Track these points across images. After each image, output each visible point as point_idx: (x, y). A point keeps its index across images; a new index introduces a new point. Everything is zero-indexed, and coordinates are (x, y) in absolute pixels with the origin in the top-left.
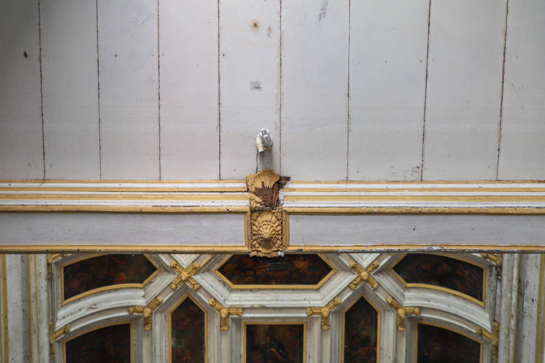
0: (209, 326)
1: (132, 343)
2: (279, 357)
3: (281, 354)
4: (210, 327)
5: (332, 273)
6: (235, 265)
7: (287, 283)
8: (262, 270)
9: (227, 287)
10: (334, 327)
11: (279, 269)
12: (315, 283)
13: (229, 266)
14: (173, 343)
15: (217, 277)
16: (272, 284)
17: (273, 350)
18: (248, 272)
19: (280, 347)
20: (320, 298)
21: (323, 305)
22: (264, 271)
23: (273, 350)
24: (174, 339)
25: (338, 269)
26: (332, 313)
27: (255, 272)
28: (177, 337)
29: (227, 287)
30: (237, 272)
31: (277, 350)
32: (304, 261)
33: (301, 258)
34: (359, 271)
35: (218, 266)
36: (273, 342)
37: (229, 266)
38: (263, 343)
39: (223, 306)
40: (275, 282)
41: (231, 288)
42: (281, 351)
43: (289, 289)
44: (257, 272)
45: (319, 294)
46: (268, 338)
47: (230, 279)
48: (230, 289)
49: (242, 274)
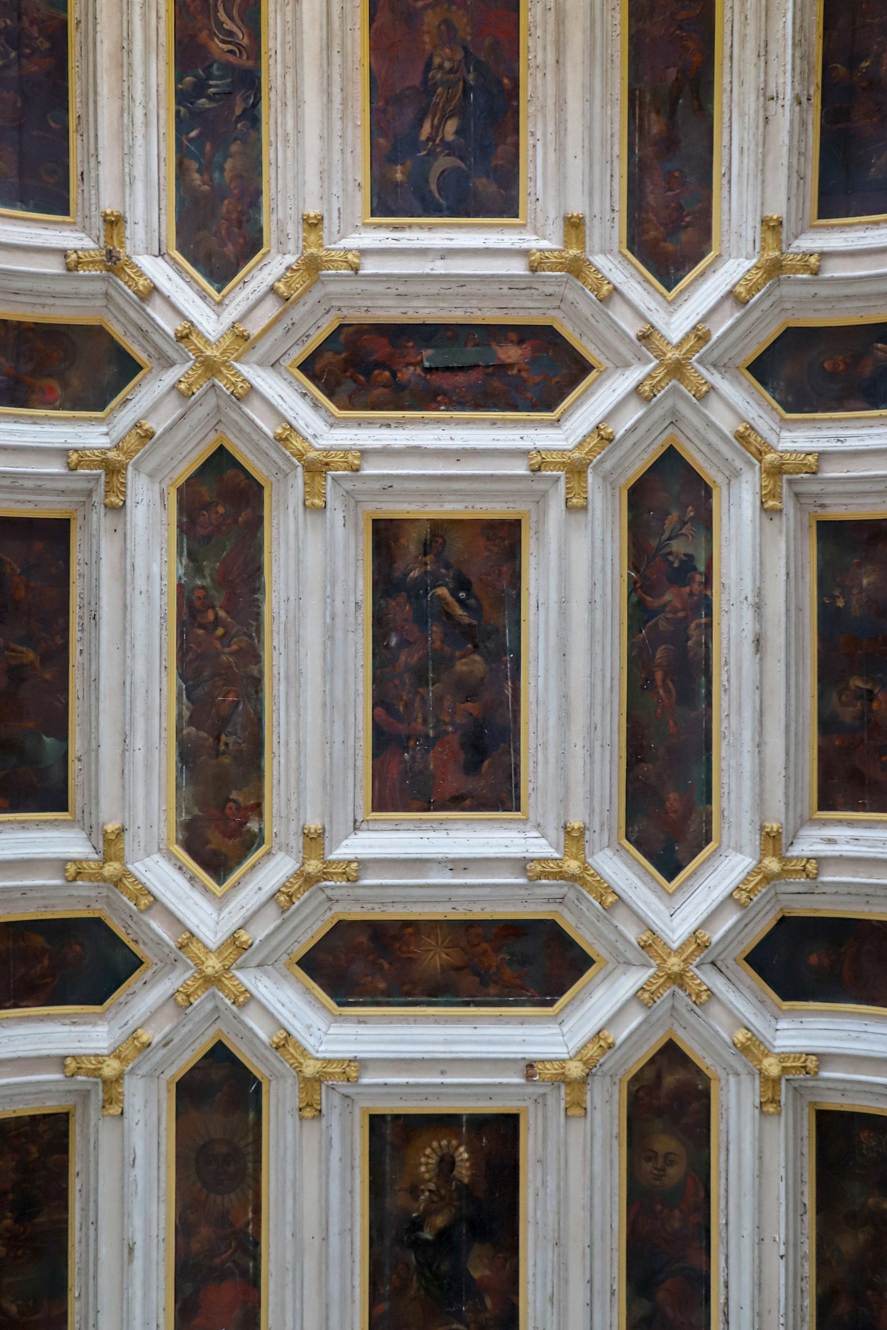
0: (275, 522)
1: (75, 569)
2: (459, 611)
3: (461, 602)
4: (278, 524)
5: (593, 374)
6: (343, 355)
7: (477, 407)
8: (411, 369)
9: (323, 412)
10: (598, 513)
11: (455, 365)
12: (550, 408)
13: (329, 356)
14: (181, 572)
15: (295, 384)
16: (437, 409)
17: (443, 591)
18: (376, 372)
19: (462, 584)
20: (563, 437)
21: (570, 447)
22: (419, 370)
23: (443, 591)
24: (185, 560)
25: (608, 364)
26: (594, 468)
27: (394, 375)
28: (192, 556)
29: (323, 412)
30: (348, 374)
31: (454, 594)
32: (520, 342)
33: (513, 336)
34: (661, 350)
35: (301, 353)
36: (443, 571)
37: (329, 356)
38: (415, 574)
39: (310, 444)
40: (445, 404)
41: (333, 415)
42: (462, 595)
43: (483, 420)
44: (399, 375)
45: (559, 431)
46: (428, 559)
47: (330, 395)
48: (331, 420)
49: (362, 378)
